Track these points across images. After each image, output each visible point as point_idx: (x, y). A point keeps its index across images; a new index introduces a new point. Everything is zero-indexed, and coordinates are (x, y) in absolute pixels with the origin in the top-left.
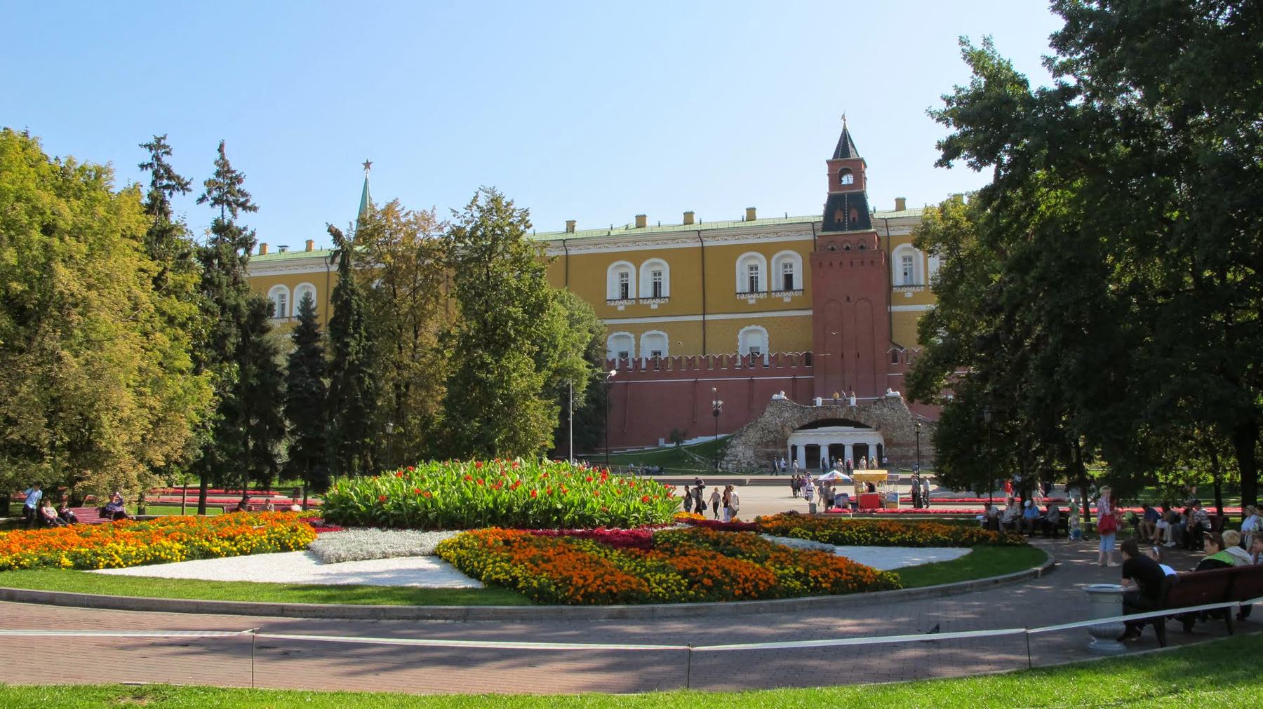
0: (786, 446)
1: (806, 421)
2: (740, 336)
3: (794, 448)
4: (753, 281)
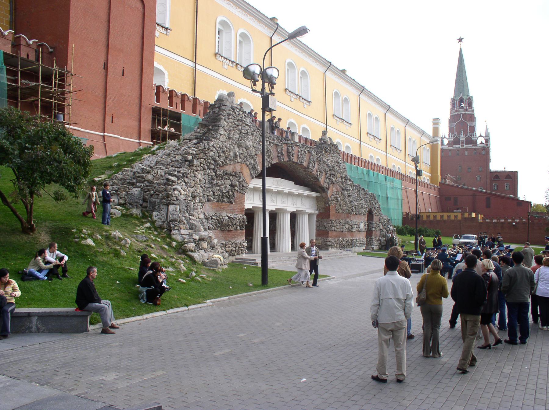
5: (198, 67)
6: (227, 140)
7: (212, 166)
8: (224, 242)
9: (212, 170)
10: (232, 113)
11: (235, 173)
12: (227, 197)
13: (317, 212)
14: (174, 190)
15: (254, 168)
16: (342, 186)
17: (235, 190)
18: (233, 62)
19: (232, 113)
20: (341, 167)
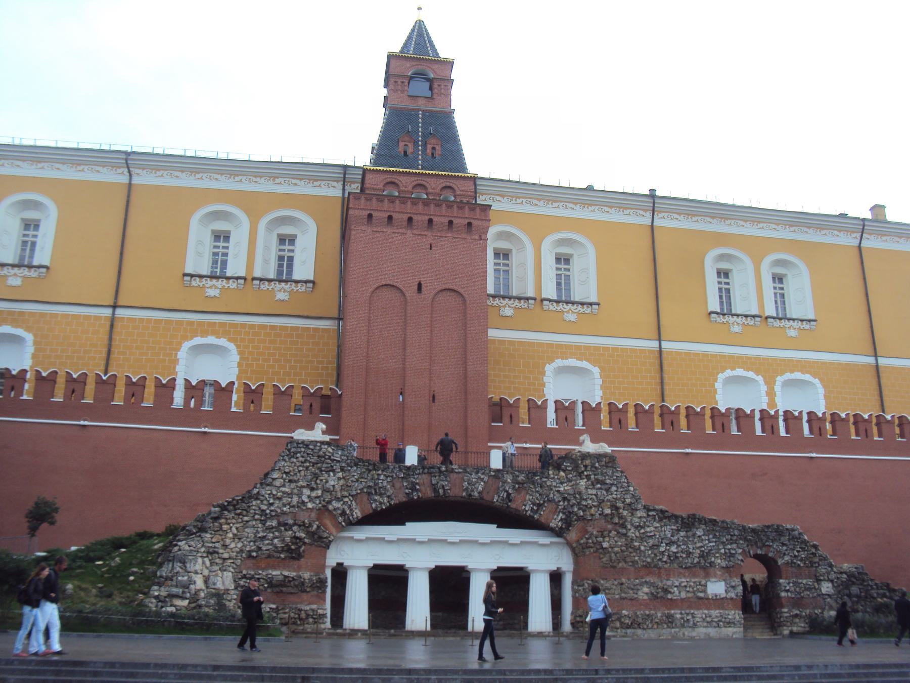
1: (382, 502)
2: (182, 354)
3: (340, 574)
4: (220, 259)
5: (665, 345)
6: (287, 484)
7: (257, 517)
8: (274, 606)
10: (303, 450)
13: (571, 569)
14: (176, 545)
15: (343, 513)
16: (616, 520)
17: (305, 543)
18: (754, 316)
20: (614, 488)
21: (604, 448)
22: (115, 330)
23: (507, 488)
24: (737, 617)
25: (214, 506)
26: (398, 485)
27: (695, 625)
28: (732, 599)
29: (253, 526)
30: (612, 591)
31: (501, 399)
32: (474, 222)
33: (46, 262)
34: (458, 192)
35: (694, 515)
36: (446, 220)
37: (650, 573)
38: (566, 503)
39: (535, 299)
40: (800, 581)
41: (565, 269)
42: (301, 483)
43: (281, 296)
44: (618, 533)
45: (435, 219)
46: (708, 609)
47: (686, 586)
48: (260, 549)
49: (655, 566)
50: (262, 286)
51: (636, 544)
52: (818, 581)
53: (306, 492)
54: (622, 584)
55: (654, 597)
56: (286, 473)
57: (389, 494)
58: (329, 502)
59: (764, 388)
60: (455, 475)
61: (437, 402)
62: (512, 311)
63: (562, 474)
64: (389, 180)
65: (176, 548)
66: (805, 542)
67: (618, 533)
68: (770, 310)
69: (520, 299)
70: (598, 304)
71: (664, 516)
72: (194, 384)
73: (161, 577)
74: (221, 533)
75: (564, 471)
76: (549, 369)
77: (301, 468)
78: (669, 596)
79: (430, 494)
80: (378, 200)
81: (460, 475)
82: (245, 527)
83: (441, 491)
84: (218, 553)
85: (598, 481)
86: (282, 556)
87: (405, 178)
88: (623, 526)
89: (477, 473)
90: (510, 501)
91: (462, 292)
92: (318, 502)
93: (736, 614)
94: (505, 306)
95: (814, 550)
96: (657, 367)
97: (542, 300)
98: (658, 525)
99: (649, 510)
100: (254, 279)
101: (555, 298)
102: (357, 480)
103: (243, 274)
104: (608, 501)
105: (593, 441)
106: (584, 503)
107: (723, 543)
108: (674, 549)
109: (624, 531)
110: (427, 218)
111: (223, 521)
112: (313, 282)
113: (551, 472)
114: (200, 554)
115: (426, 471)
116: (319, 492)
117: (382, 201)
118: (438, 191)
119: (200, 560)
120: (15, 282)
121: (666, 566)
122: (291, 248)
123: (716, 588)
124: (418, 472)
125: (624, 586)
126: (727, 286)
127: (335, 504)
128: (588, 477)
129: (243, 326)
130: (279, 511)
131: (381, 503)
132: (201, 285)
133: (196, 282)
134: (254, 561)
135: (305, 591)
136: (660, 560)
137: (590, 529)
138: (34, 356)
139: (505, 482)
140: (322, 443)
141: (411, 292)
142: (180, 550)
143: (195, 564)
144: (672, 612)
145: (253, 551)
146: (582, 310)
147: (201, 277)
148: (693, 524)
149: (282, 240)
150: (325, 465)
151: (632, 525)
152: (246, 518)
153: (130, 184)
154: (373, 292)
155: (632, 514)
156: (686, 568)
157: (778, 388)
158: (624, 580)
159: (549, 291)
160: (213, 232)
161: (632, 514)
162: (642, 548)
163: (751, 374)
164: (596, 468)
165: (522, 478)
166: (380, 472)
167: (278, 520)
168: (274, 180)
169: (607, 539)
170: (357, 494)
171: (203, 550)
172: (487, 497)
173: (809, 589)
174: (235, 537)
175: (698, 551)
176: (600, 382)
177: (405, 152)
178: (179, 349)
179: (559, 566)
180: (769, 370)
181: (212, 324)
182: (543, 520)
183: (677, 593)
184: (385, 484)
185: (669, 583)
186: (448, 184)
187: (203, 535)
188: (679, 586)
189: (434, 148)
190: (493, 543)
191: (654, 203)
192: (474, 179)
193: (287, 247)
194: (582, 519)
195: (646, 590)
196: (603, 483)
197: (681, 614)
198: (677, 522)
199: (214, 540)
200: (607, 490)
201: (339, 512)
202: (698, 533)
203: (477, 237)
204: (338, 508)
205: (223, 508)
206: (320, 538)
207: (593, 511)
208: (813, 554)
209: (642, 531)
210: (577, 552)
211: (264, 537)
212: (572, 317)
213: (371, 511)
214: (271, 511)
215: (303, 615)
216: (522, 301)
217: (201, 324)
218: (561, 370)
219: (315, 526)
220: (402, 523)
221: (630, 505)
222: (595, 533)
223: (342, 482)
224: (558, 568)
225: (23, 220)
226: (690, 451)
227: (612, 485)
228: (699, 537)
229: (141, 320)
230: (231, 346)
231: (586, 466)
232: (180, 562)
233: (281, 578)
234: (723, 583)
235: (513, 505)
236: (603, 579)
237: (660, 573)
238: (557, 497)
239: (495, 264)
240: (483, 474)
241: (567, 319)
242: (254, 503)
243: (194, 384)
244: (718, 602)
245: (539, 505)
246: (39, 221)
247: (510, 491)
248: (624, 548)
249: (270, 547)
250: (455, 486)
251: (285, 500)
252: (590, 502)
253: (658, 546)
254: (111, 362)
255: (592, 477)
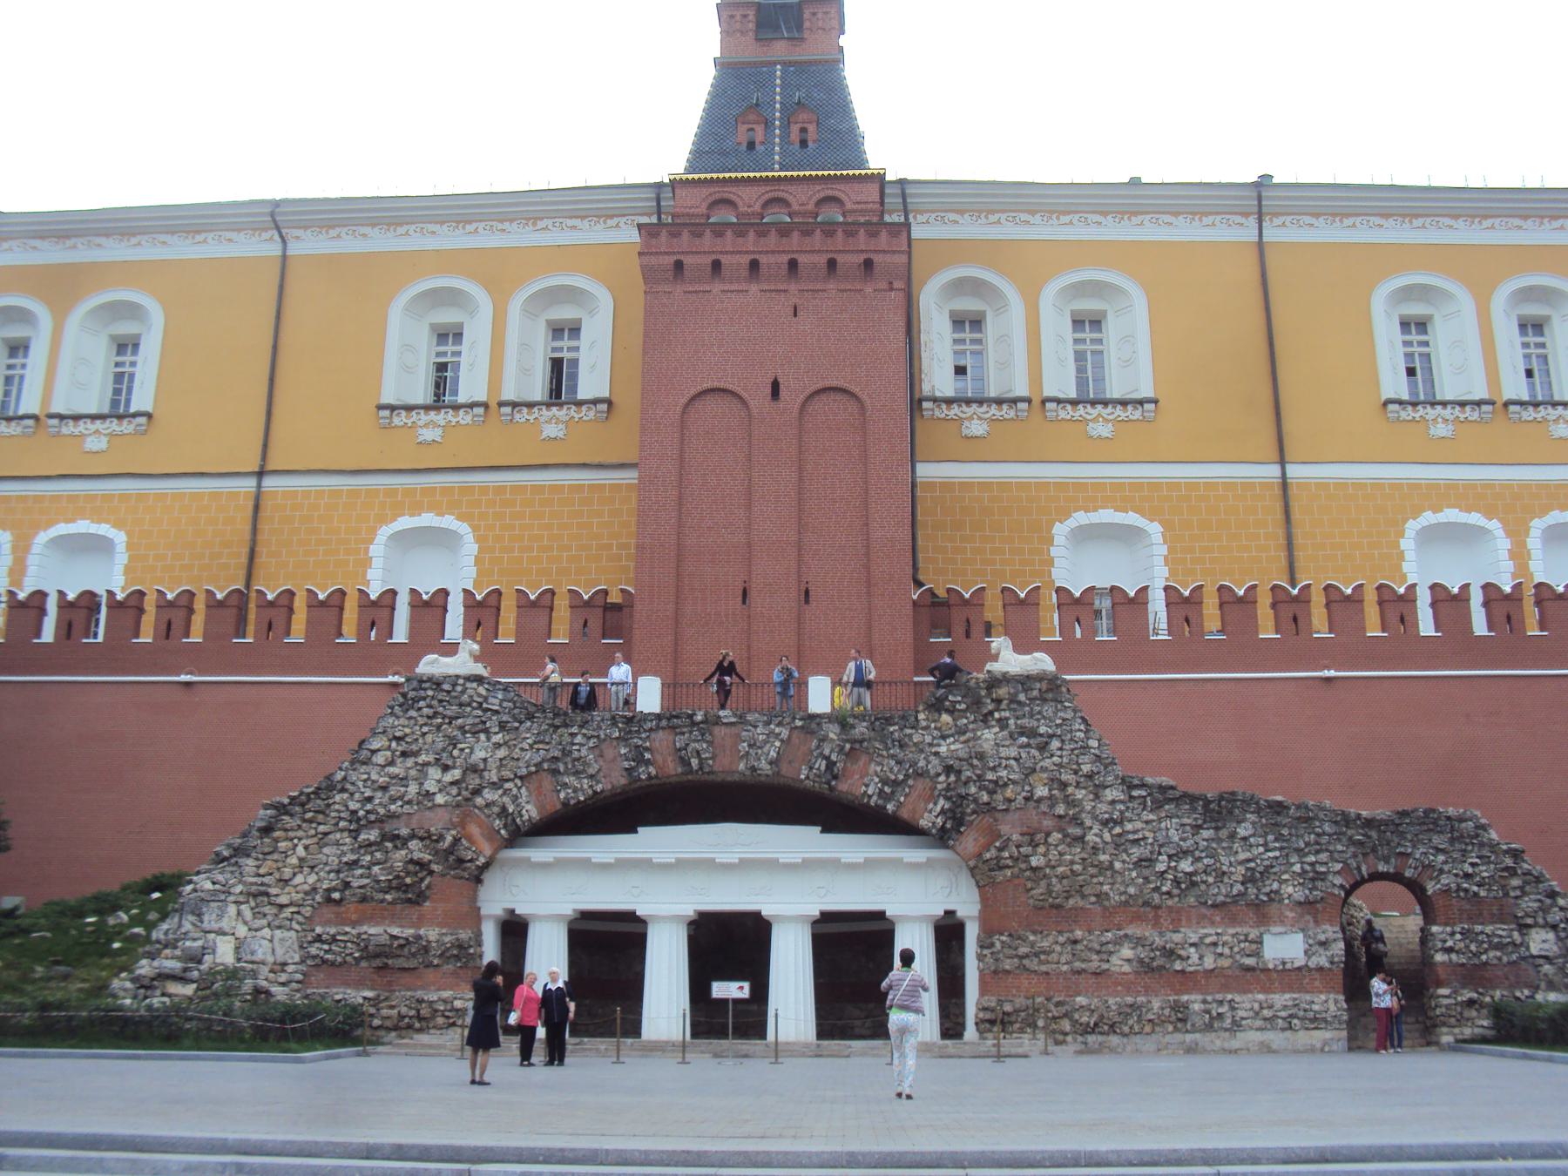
0: (476, 917)
1: (577, 789)
2: (377, 549)
3: (514, 930)
4: (443, 376)
5: (1293, 471)
7: (342, 824)
8: (370, 994)
9: (346, 834)
10: (430, 693)
11: (428, 831)
12: (398, 889)
16: (1060, 809)
17: (431, 873)
18: (1479, 403)
19: (430, 693)
20: (1055, 744)
21: (1041, 662)
22: (261, 514)
23: (827, 752)
24: (1332, 1007)
25: (266, 807)
26: (609, 753)
27: (1237, 1026)
28: (1320, 969)
29: (337, 843)
30: (1054, 957)
31: (949, 590)
32: (877, 258)
33: (149, 409)
34: (849, 206)
35: (1233, 793)
36: (822, 260)
37: (1137, 918)
38: (952, 778)
39: (1029, 401)
40: (1478, 928)
41: (1093, 341)
42: (423, 758)
43: (551, 431)
44: (1066, 836)
45: (802, 259)
46: (1266, 990)
47: (1215, 944)
48: (347, 885)
49: (1146, 903)
50: (517, 416)
51: (1103, 857)
52: (1523, 928)
53: (435, 773)
54: (1075, 942)
55: (1146, 968)
56: (398, 739)
57: (591, 771)
58: (477, 792)
59: (1504, 544)
60: (724, 730)
61: (813, 604)
62: (985, 426)
63: (946, 718)
64: (718, 196)
65: (189, 888)
66: (1493, 847)
67: (1066, 836)
68: (1514, 386)
69: (999, 402)
70: (1156, 402)
71: (1163, 797)
72: (373, 597)
73: (158, 942)
74: (275, 856)
75: (951, 712)
76: (1060, 531)
77: (425, 729)
78: (1178, 966)
79: (673, 769)
80: (693, 234)
81: (734, 730)
82: (321, 845)
83: (694, 762)
84: (267, 894)
85: (1023, 732)
86: (388, 897)
87: (748, 189)
88: (1076, 820)
89: (768, 723)
90: (835, 777)
91: (856, 390)
92: (454, 791)
93: (1331, 1003)
94: (970, 418)
95: (1509, 862)
96: (1280, 516)
97: (1044, 402)
98: (1151, 817)
99: (1131, 787)
100: (501, 404)
101: (1073, 395)
102: (531, 746)
103: (482, 397)
104: (1044, 769)
105: (1020, 648)
106: (990, 776)
107: (1298, 850)
108: (1186, 865)
109: (1077, 831)
110: (785, 258)
111: (277, 834)
112: (609, 402)
113: (921, 716)
114: (232, 898)
115: (664, 723)
116: (456, 774)
117: (700, 235)
118: (811, 207)
119: (232, 909)
120: (95, 444)
121: (1170, 903)
122: (574, 343)
123: (1285, 946)
124: (648, 725)
125: (1079, 947)
126: (1424, 350)
127: (489, 795)
128: (1002, 723)
129: (484, 490)
130: (382, 811)
131: (575, 790)
132: (410, 423)
133: (401, 419)
134: (336, 909)
135: (429, 965)
136: (1157, 889)
137: (1005, 829)
138: (128, 570)
139: (824, 739)
140: (468, 679)
141: (758, 398)
142: (195, 890)
143: (220, 917)
144: (1185, 998)
145: (334, 889)
146: (1123, 415)
147: (409, 408)
148: (1230, 812)
149: (557, 331)
150: (470, 721)
151: (1095, 818)
152: (322, 828)
153: (284, 257)
154: (687, 406)
155: (1097, 797)
156: (1214, 906)
157: (1534, 542)
158: (1079, 934)
159: (1060, 381)
160: (433, 327)
161: (1097, 797)
162: (1118, 865)
163: (1475, 518)
164: (1019, 703)
165: (861, 729)
166: (575, 730)
167: (381, 829)
168: (534, 224)
169: (1041, 849)
170: (530, 774)
171: (239, 888)
172: (786, 770)
173: (1500, 947)
174: (308, 863)
175: (1241, 869)
176: (1164, 550)
177: (751, 145)
178: (371, 541)
179: (950, 907)
180: (1514, 508)
181: (429, 491)
182: (905, 814)
183: (1195, 957)
184: (584, 752)
185: (1177, 937)
186: (830, 193)
187: (242, 861)
188: (1201, 943)
189: (803, 130)
190: (807, 865)
191: (1260, 199)
192: (880, 178)
193: (566, 343)
194: (989, 808)
195: (1127, 952)
196: (1032, 733)
197: (1204, 1002)
198: (1194, 810)
199: (262, 871)
200: (1043, 748)
201: (496, 809)
202: (1242, 832)
203: (884, 285)
204: (493, 803)
205: (281, 809)
206: (461, 861)
207: (1009, 793)
208: (1507, 869)
209: (1118, 830)
210: (984, 873)
211: (355, 862)
212: (1104, 430)
213: (559, 806)
214: (368, 812)
215: (425, 1012)
216: (1005, 407)
217: (409, 492)
218: (1085, 535)
219: (449, 839)
220: (632, 830)
221: (1090, 776)
222: (1015, 837)
223: (502, 753)
224: (950, 913)
225: (113, 338)
226: (1332, 673)
227: (1051, 736)
228: (1245, 839)
229: (306, 494)
230: (463, 528)
231: (998, 701)
232: (193, 913)
233: (385, 939)
234: (1301, 935)
235: (843, 787)
236: (1034, 932)
237: (1157, 917)
238: (935, 766)
239: (956, 341)
240: (779, 724)
241: (1094, 433)
242: (338, 798)
243: (373, 597)
244: (1289, 977)
245: (895, 783)
246: (138, 336)
247: (834, 757)
248: (1077, 867)
249: (366, 881)
250: (757, 750)
251: (393, 791)
252: (1004, 773)
253: (1150, 861)
254: (255, 572)
255: (1011, 722)
